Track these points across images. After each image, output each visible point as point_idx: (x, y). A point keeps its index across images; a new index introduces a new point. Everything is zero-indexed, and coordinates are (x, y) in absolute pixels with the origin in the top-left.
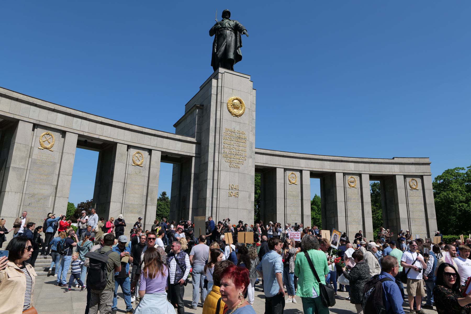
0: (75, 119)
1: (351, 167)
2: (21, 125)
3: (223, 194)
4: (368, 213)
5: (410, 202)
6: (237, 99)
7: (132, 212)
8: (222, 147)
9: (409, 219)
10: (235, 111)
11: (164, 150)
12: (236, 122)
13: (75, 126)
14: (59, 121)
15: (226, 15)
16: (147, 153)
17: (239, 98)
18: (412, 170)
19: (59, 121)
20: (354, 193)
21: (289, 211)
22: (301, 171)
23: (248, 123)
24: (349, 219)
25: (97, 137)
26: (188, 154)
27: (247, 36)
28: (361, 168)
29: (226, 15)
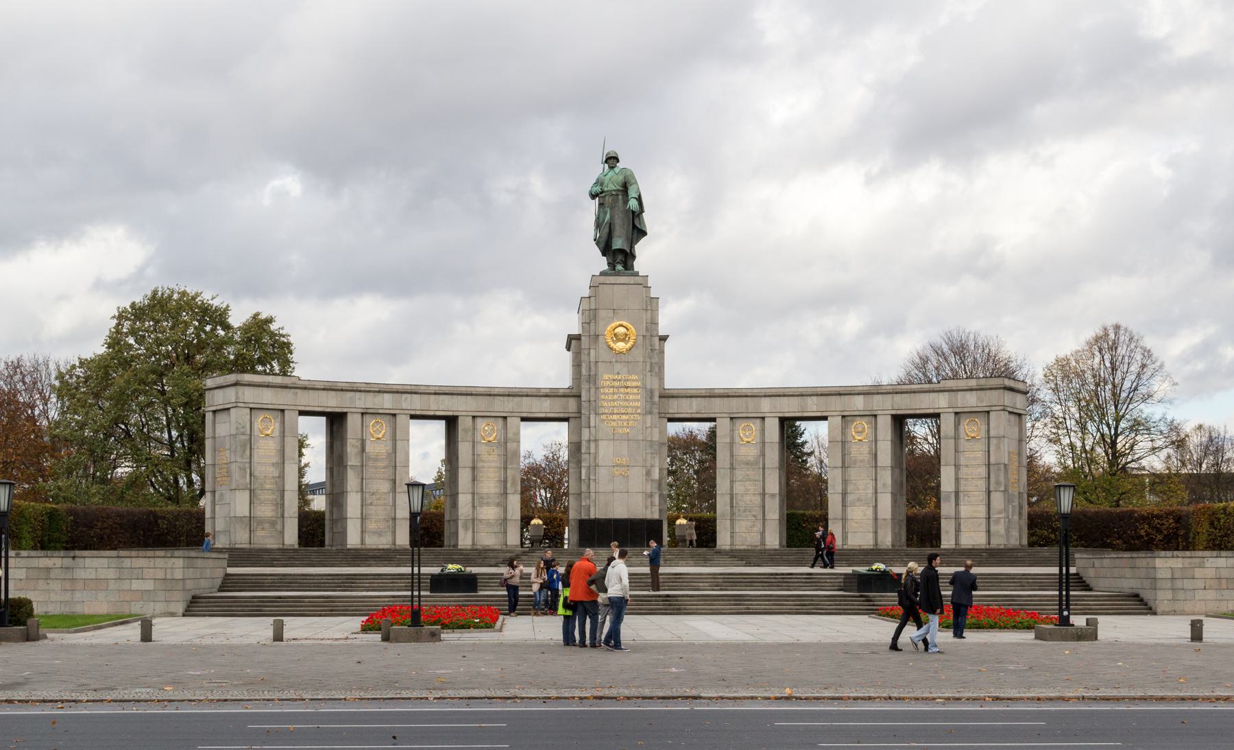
0: (404, 396)
1: (859, 403)
2: (349, 417)
3: (603, 473)
4: (884, 485)
5: (963, 461)
6: (621, 326)
7: (488, 504)
9: (957, 493)
10: (621, 346)
11: (525, 415)
13: (404, 406)
14: (387, 402)
15: (612, 160)
16: (500, 421)
17: (624, 323)
18: (971, 401)
19: (387, 402)
20: (860, 452)
21: (738, 488)
22: (763, 418)
24: (850, 498)
25: (431, 413)
28: (878, 403)
29: (612, 160)
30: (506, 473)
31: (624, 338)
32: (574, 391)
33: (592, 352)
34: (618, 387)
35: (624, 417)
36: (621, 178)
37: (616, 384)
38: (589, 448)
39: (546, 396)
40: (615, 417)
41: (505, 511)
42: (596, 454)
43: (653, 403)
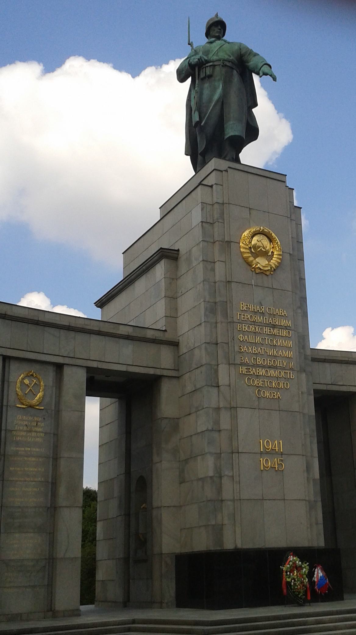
8: (237, 349)
11: (95, 365)
12: (263, 287)
15: (216, 28)
23: (290, 288)
26: (151, 371)
27: (275, 79)
29: (216, 28)
30: (56, 466)
31: (265, 254)
32: (168, 336)
33: (219, 267)
34: (261, 325)
35: (272, 372)
36: (236, 47)
37: (259, 319)
38: (217, 422)
39: (127, 337)
40: (262, 372)
41: (52, 543)
42: (233, 432)
43: (306, 358)
